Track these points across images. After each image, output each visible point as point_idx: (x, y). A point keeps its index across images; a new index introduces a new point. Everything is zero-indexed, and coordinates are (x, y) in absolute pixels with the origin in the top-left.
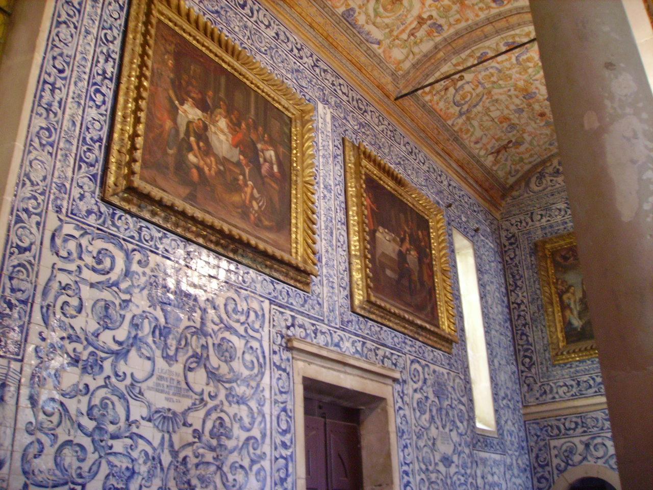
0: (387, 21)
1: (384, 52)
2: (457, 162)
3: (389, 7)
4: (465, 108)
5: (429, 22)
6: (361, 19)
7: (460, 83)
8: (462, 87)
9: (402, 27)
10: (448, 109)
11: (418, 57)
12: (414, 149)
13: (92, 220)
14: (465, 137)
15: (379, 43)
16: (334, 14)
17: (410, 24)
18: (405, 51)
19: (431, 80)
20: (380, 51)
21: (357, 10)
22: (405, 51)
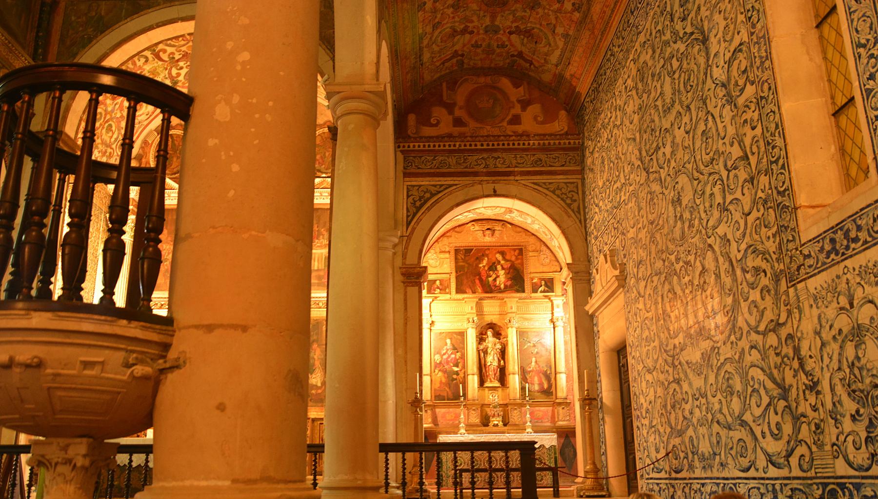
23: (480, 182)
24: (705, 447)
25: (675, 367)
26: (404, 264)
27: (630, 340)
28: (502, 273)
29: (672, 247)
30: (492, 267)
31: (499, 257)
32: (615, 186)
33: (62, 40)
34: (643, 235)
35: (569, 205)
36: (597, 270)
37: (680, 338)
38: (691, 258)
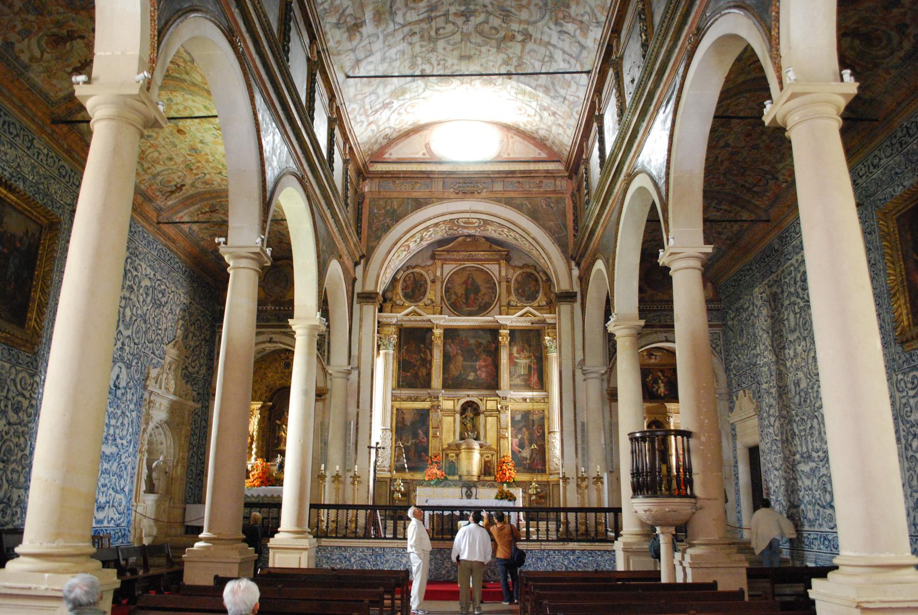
13: (905, 366)
23: (656, 332)
24: (811, 515)
25: (794, 471)
26: (609, 387)
27: (762, 447)
28: (662, 385)
29: (793, 407)
30: (655, 381)
31: (660, 374)
32: (753, 352)
33: (370, 227)
34: (773, 390)
35: (714, 349)
36: (737, 397)
37: (798, 457)
38: (805, 418)
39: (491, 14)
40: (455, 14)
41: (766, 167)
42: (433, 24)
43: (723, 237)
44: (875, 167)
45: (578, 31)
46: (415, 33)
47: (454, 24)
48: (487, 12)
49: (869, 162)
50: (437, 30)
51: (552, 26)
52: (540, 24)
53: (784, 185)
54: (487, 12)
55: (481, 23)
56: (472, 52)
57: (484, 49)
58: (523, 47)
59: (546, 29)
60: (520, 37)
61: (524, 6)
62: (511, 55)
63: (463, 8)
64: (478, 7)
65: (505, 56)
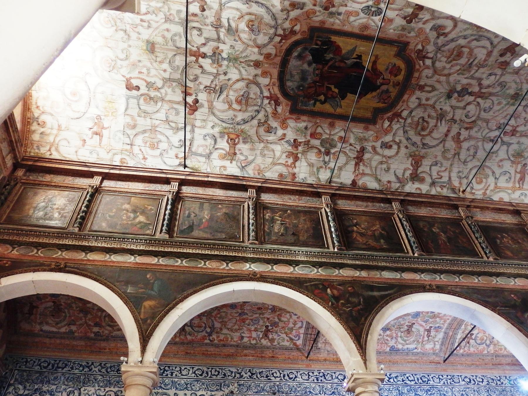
0: (412, 340)
1: (421, 349)
2: (508, 364)
3: (408, 335)
4: (488, 342)
5: (432, 329)
6: (400, 347)
7: (473, 337)
8: (476, 337)
9: (422, 337)
10: (478, 348)
11: (440, 342)
12: (471, 377)
14: (502, 352)
15: (416, 348)
16: (386, 353)
17: (424, 334)
18: (432, 343)
19: (456, 345)
20: (419, 350)
21: (395, 345)
22: (432, 343)
39: (215, 77)
40: (218, 48)
41: (217, 325)
42: (210, 27)
43: (96, 329)
44: (290, 379)
45: (224, 152)
46: (203, 10)
47: (204, 44)
48: (218, 74)
49: (285, 373)
50: (200, 30)
51: (217, 129)
52: (212, 118)
53: (207, 341)
54: (218, 74)
55: (201, 67)
56: (161, 57)
57: (165, 66)
58: (178, 103)
59: (211, 124)
60: (190, 100)
61: (230, 106)
62: (163, 91)
63: (225, 55)
64: (224, 67)
65: (160, 86)
